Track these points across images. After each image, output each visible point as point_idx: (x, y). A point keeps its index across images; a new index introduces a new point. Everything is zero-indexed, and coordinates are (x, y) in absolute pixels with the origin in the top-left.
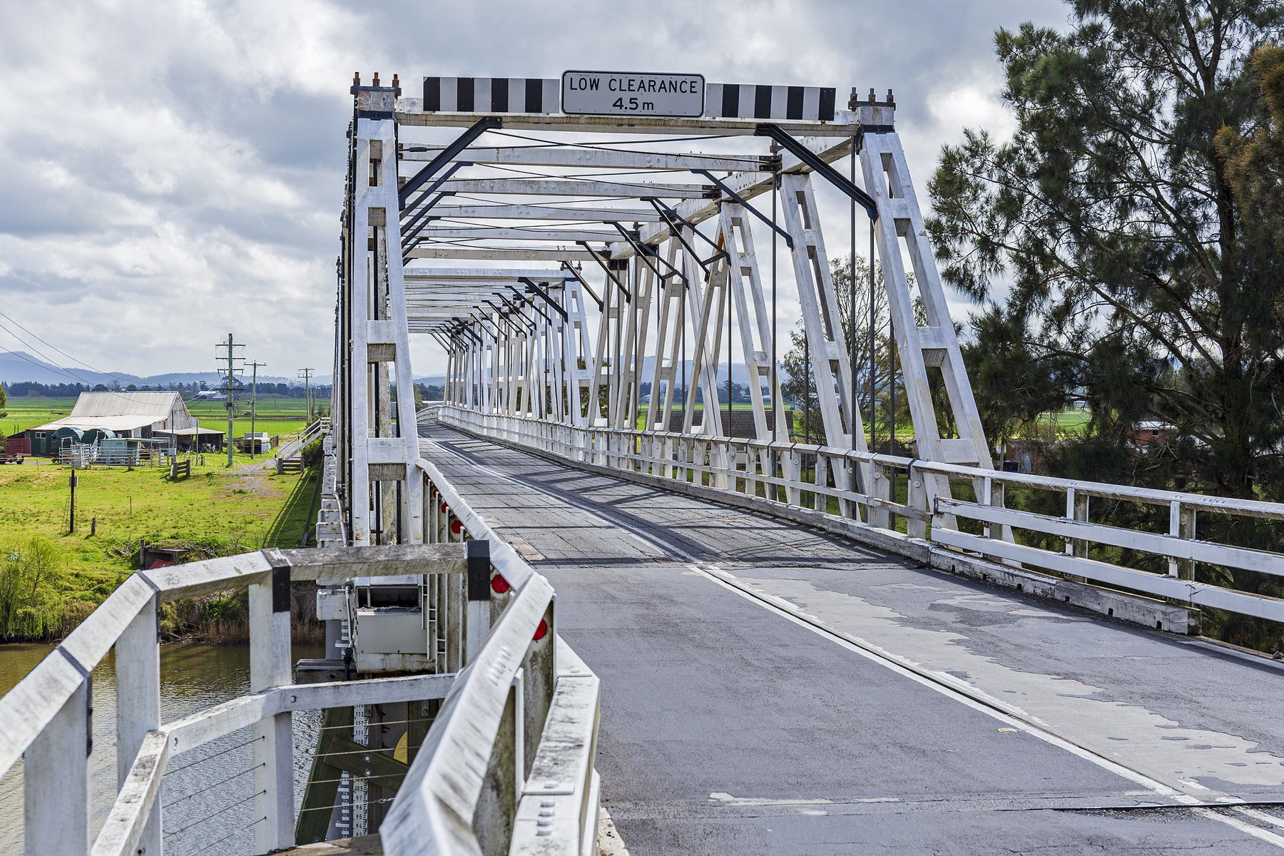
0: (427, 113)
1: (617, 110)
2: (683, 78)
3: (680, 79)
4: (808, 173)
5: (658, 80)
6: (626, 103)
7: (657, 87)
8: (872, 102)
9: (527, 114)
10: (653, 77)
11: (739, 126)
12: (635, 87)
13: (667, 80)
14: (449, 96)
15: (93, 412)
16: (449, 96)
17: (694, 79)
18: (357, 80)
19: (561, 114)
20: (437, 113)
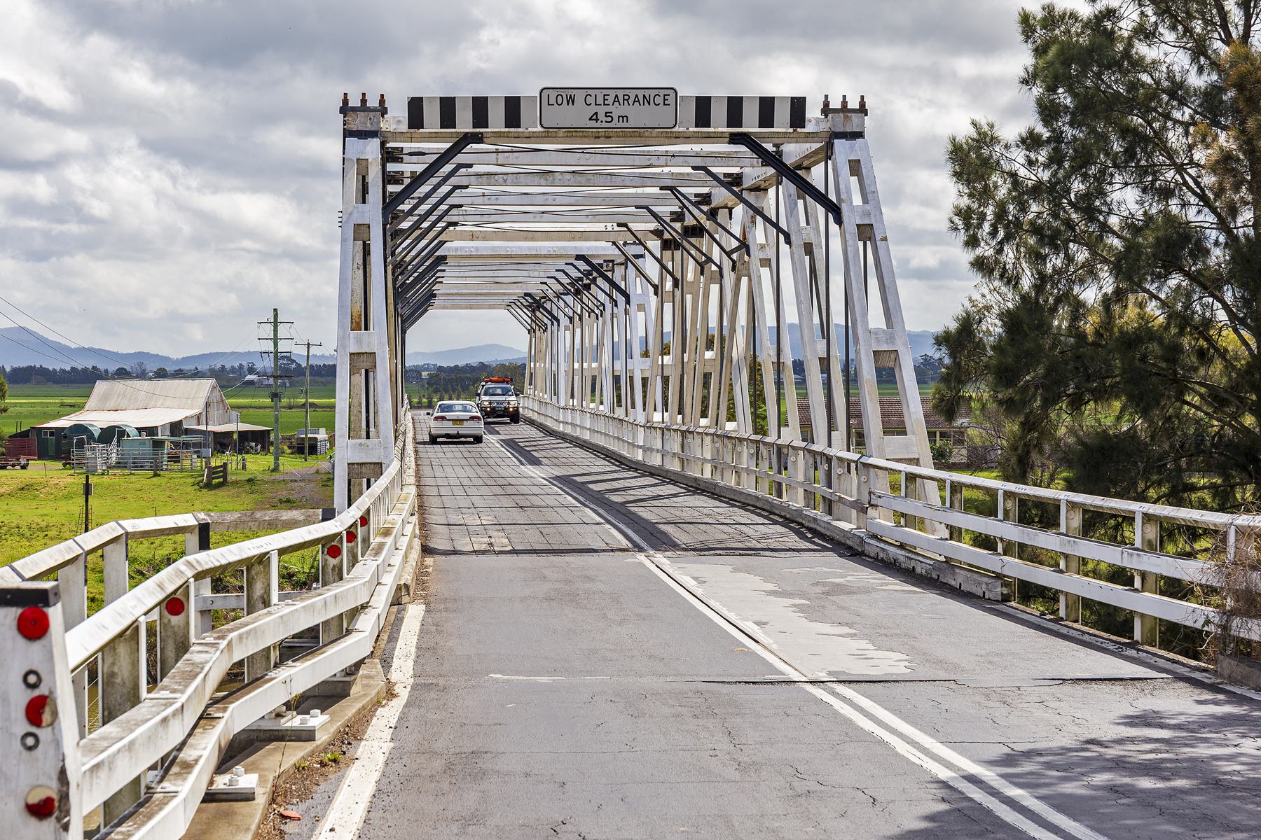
1: (593, 124)
2: (656, 92)
3: (653, 93)
5: (632, 94)
6: (601, 117)
7: (631, 102)
8: (844, 108)
9: (507, 130)
10: (627, 92)
11: (711, 135)
13: (640, 94)
14: (432, 115)
15: (111, 405)
16: (432, 115)
17: (666, 92)
18: (345, 101)
19: (539, 129)
20: (421, 130)
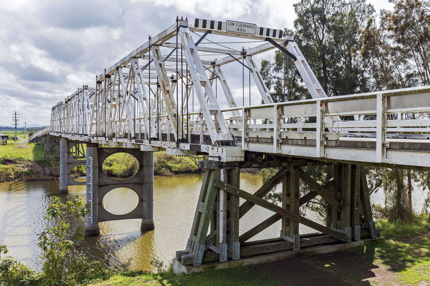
0: (195, 28)
1: (238, 31)
2: (252, 25)
3: (252, 25)
4: (251, 56)
6: (240, 30)
7: (246, 27)
9: (218, 30)
10: (246, 24)
11: (262, 38)
12: (242, 26)
13: (249, 25)
14: (201, 24)
16: (201, 24)
17: (254, 25)
18: (177, 18)
19: (226, 31)
20: (197, 28)
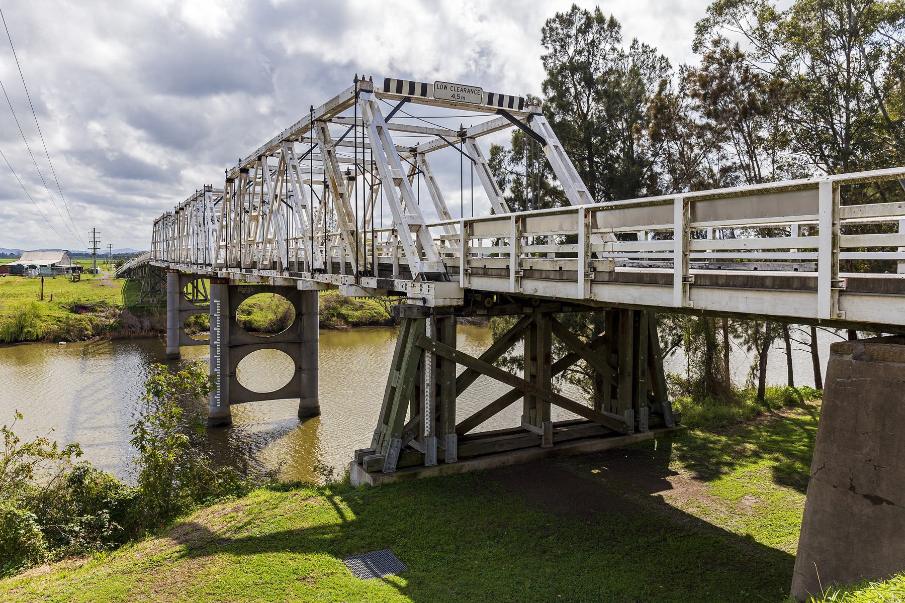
1: (452, 99)
4: (474, 138)
5: (467, 88)
6: (456, 96)
10: (465, 87)
13: (470, 88)
14: (393, 86)
16: (393, 86)
18: (356, 77)
